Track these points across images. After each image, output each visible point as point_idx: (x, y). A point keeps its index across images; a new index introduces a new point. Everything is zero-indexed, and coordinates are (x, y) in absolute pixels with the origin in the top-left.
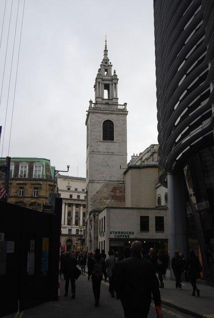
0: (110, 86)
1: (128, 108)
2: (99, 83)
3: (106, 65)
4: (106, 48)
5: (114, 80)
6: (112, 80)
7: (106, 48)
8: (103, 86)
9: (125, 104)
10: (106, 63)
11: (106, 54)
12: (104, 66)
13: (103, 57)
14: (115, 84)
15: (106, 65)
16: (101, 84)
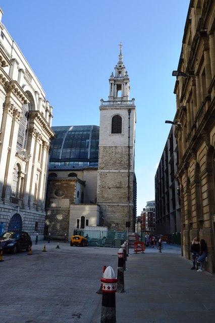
0: (122, 85)
1: (136, 103)
2: (112, 84)
3: (120, 68)
4: (121, 53)
5: (126, 79)
6: (124, 80)
7: (121, 53)
8: (116, 86)
9: (133, 99)
10: (120, 66)
11: (121, 59)
12: (118, 69)
13: (118, 61)
14: (126, 83)
15: (120, 68)
16: (113, 84)
